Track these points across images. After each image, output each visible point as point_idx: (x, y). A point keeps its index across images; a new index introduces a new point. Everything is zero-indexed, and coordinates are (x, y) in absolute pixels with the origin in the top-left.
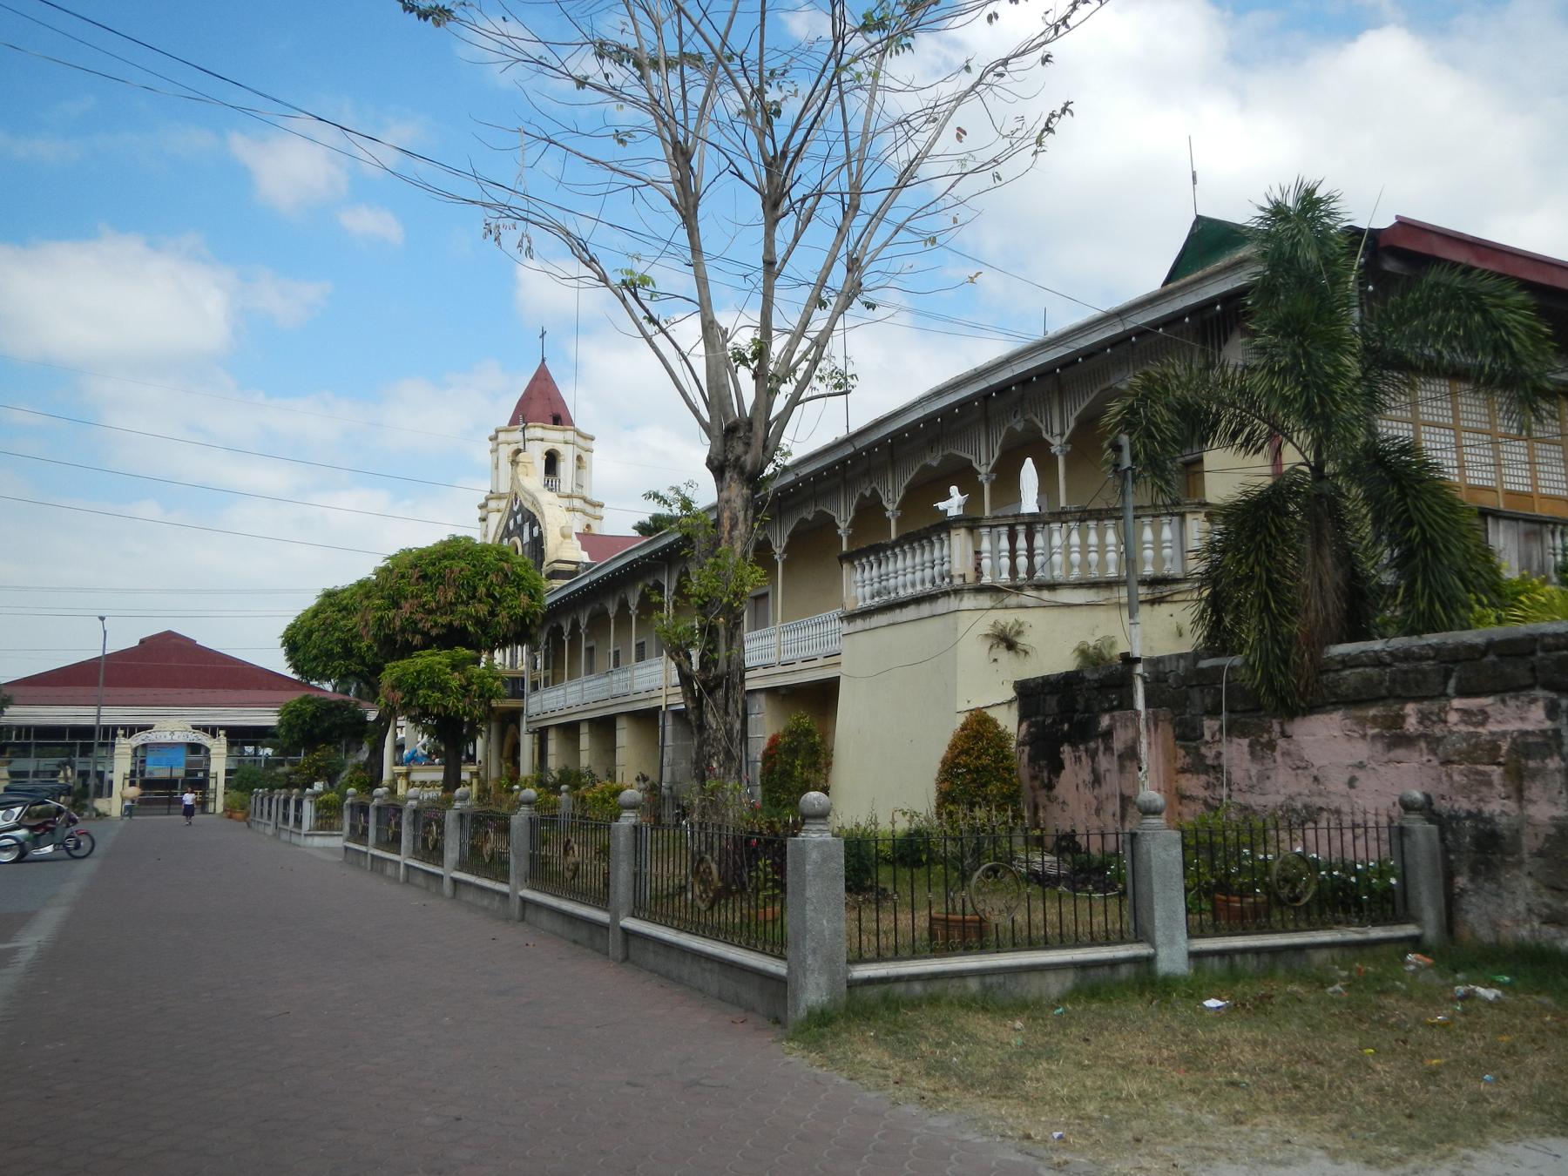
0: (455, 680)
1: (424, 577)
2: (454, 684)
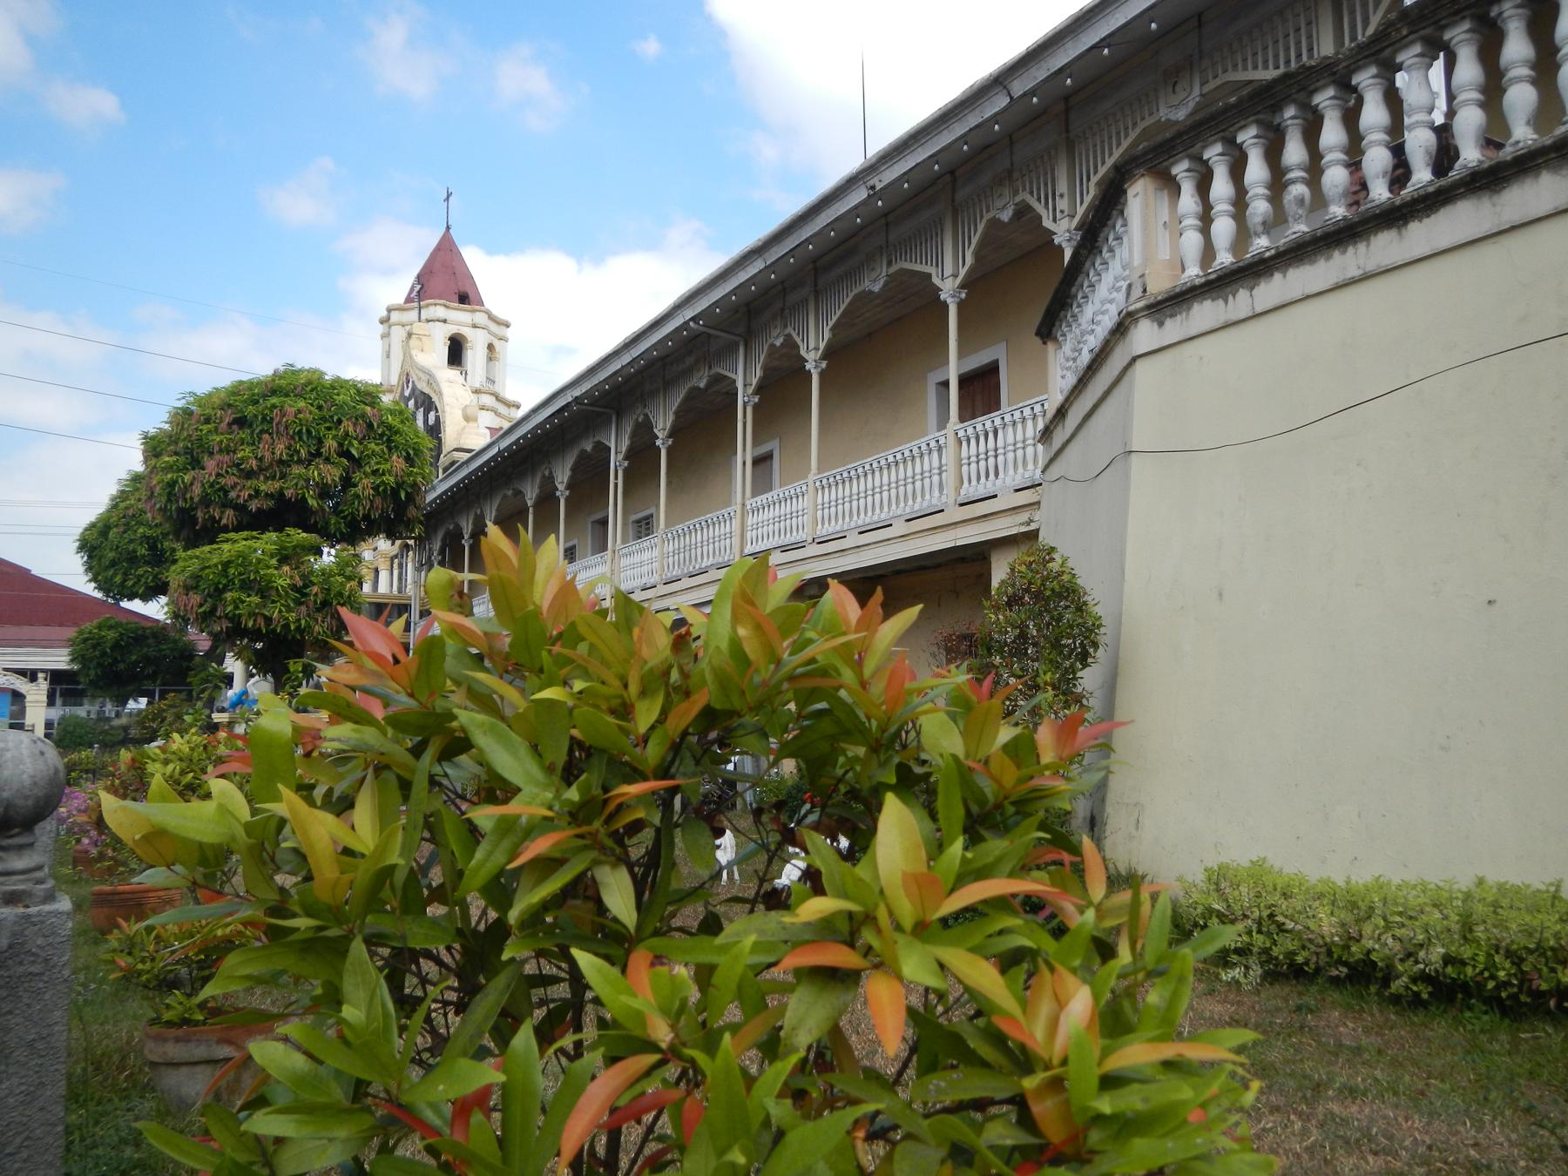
0: (283, 578)
1: (241, 422)
2: (282, 582)
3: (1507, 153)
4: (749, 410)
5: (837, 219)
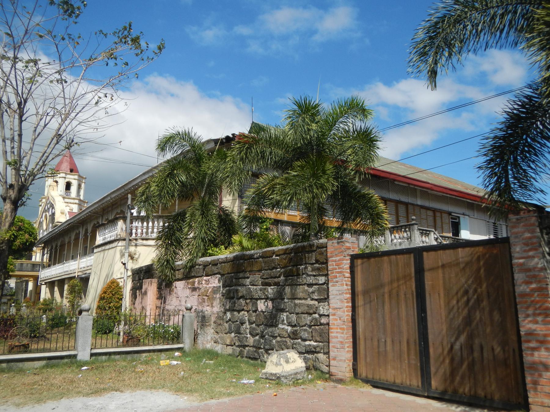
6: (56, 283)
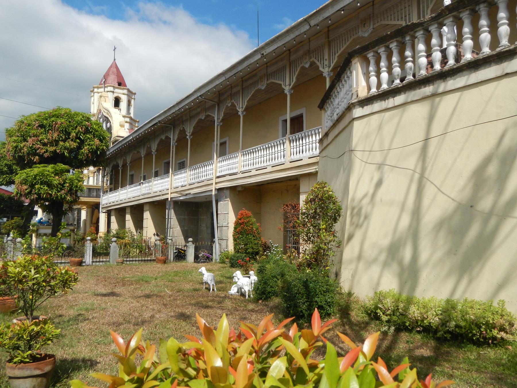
0: (56, 180)
1: (42, 126)
2: (55, 182)
3: (481, 56)
4: (219, 127)
5: (250, 65)
6: (128, 210)
